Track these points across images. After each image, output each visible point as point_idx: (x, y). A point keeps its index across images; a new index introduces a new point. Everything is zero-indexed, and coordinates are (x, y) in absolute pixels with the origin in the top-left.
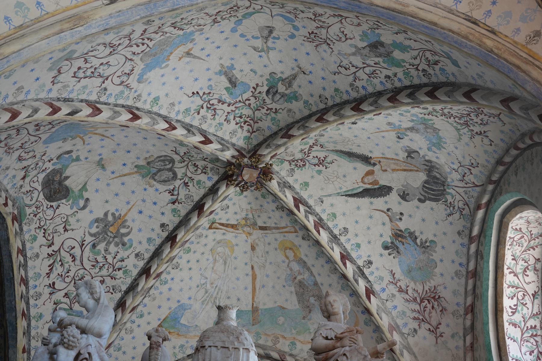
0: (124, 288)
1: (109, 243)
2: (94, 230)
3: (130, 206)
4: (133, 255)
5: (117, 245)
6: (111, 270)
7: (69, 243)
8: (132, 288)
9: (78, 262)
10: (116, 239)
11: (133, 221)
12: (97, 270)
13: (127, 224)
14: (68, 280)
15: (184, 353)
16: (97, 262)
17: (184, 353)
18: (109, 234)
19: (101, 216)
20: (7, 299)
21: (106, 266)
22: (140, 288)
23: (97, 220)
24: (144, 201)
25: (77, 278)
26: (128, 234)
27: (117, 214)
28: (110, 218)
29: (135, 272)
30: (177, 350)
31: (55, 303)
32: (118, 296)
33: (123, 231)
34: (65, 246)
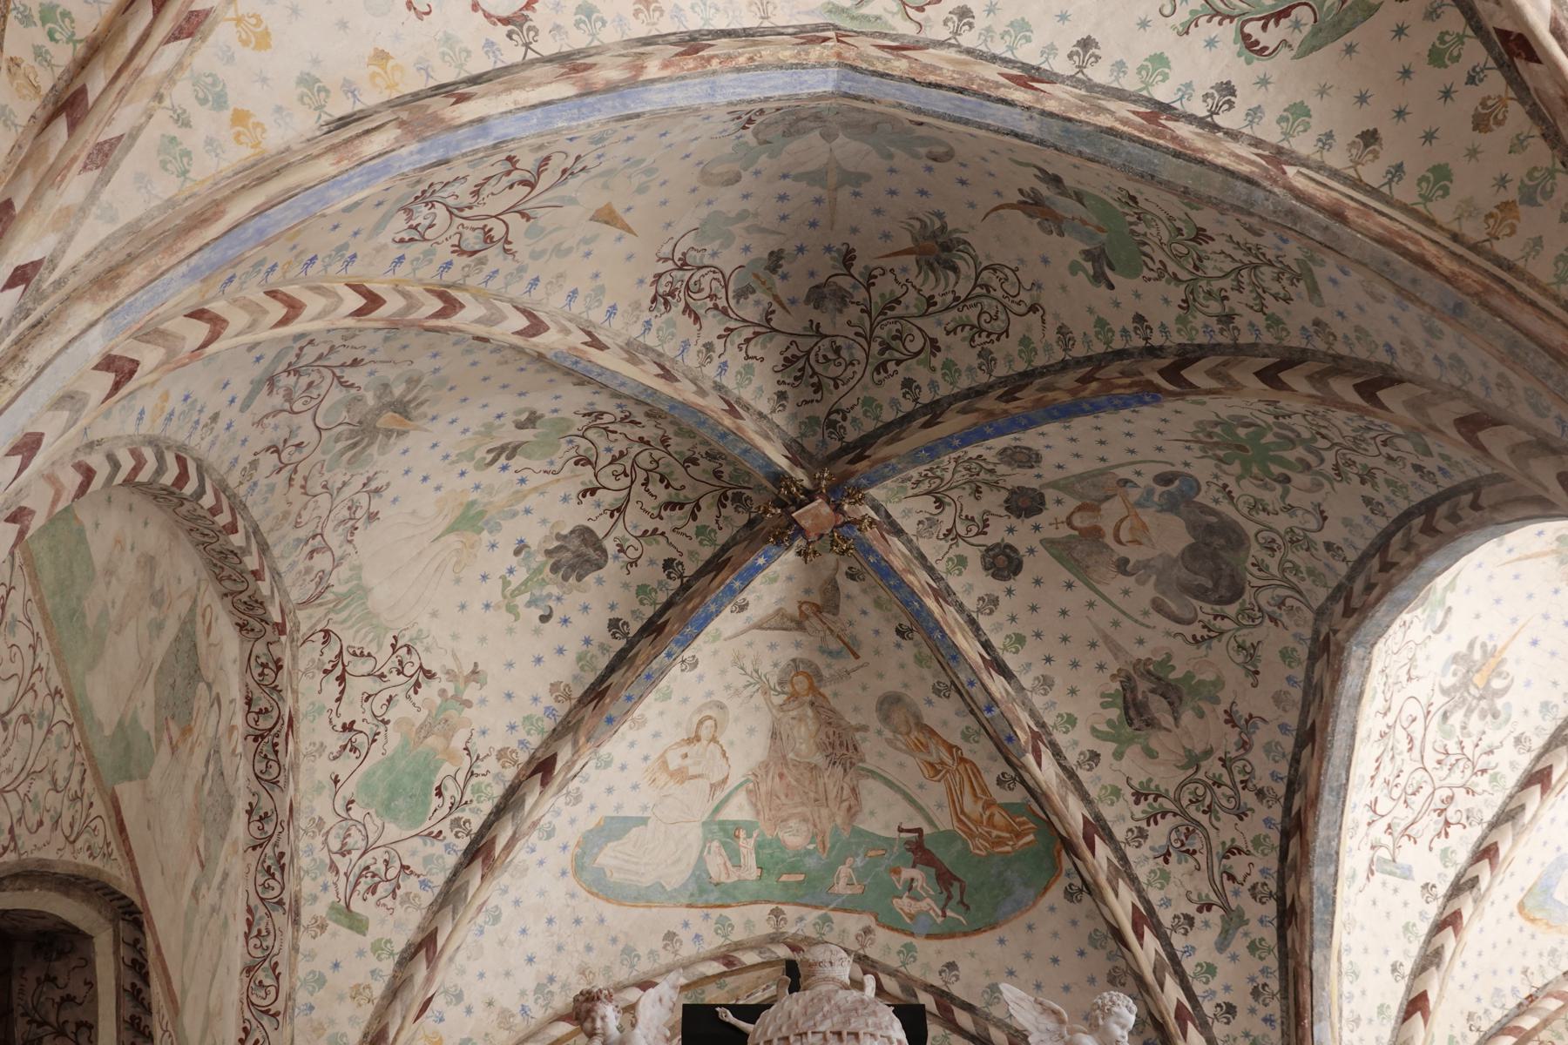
0: (1488, 815)
1: (1470, 711)
2: (1449, 681)
3: (1516, 628)
4: (1511, 740)
5: (1483, 716)
6: (1468, 772)
7: (1414, 709)
8: (1508, 815)
9: (1416, 753)
10: (1483, 704)
11: (1518, 661)
12: (1446, 769)
13: (1505, 668)
14: (1396, 793)
15: (1557, 967)
16: (1447, 754)
17: (1557, 967)
18: (1473, 690)
19: (1463, 649)
20: (1322, 833)
21: (1461, 763)
22: (1528, 815)
23: (1456, 659)
24: (1546, 617)
25: (1410, 791)
26: (1505, 690)
27: (1490, 647)
28: (1477, 655)
29: (1512, 779)
30: (1545, 961)
31: (1373, 847)
32: (1475, 832)
33: (1497, 684)
34: (1404, 716)
